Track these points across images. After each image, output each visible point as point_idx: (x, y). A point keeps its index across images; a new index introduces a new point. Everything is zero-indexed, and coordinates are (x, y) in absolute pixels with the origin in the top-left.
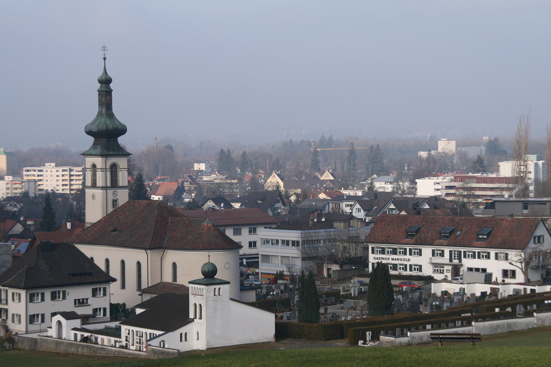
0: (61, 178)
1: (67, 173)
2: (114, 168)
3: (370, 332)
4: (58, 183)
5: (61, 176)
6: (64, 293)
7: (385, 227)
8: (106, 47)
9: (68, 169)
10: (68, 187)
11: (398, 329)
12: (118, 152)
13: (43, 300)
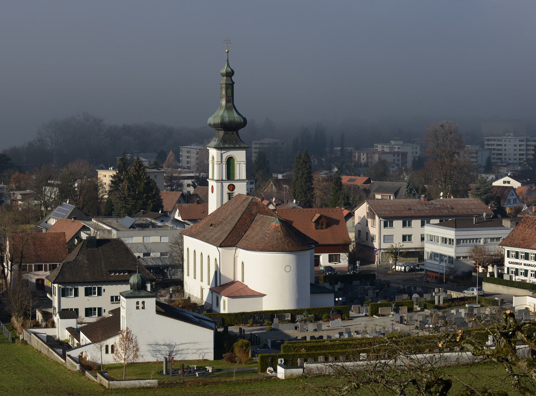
0: (518, 148)
1: (524, 143)
2: (230, 162)
3: (283, 359)
4: (515, 152)
5: (518, 146)
6: (100, 289)
7: (525, 229)
8: (230, 40)
9: (525, 139)
10: (524, 157)
11: (321, 357)
12: (234, 145)
13: (76, 295)
